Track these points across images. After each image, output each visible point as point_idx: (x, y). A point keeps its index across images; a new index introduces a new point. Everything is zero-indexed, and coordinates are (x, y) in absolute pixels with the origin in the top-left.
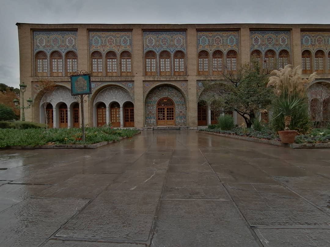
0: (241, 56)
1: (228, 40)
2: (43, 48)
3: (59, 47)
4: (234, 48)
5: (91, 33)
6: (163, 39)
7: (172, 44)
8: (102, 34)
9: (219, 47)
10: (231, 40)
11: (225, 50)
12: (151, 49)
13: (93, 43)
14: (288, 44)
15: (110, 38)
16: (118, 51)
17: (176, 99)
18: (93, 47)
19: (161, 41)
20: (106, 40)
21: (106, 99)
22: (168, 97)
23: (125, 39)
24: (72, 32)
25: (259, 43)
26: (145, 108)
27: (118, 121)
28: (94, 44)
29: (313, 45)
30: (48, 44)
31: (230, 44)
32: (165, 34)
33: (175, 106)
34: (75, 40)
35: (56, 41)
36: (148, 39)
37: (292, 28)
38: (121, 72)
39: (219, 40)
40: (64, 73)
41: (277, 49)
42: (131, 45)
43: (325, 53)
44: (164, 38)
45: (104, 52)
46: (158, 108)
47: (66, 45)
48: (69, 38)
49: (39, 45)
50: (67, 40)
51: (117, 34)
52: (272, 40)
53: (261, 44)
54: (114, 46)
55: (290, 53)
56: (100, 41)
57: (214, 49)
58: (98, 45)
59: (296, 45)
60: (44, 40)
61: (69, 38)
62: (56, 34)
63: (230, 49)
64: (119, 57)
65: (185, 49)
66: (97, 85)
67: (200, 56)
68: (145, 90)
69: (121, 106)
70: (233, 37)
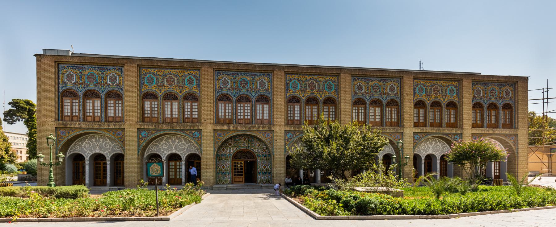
0: (340, 104)
4: (332, 95)
5: (143, 70)
6: (242, 81)
9: (314, 93)
10: (328, 86)
11: (321, 97)
12: (225, 91)
13: (145, 82)
14: (398, 94)
15: (170, 76)
17: (257, 151)
18: (146, 87)
19: (239, 83)
22: (248, 149)
23: (190, 79)
24: (116, 67)
25: (363, 91)
26: (217, 161)
27: (178, 177)
28: (147, 83)
29: (427, 95)
31: (327, 90)
32: (244, 75)
33: (256, 159)
36: (221, 80)
37: (403, 75)
38: (184, 119)
39: (314, 85)
40: (103, 118)
41: (384, 98)
42: (198, 85)
43: (443, 104)
45: (161, 94)
46: (233, 161)
47: (106, 83)
48: (111, 75)
50: (109, 76)
51: (179, 72)
52: (379, 88)
53: (365, 92)
54: (175, 87)
55: (400, 104)
56: (155, 80)
57: (308, 95)
58: (153, 85)
59: (408, 95)
60: (74, 75)
61: (111, 75)
62: (92, 69)
63: (327, 96)
64: (182, 99)
65: (271, 93)
67: (289, 103)
68: (217, 141)
69: (184, 158)
70: (331, 83)
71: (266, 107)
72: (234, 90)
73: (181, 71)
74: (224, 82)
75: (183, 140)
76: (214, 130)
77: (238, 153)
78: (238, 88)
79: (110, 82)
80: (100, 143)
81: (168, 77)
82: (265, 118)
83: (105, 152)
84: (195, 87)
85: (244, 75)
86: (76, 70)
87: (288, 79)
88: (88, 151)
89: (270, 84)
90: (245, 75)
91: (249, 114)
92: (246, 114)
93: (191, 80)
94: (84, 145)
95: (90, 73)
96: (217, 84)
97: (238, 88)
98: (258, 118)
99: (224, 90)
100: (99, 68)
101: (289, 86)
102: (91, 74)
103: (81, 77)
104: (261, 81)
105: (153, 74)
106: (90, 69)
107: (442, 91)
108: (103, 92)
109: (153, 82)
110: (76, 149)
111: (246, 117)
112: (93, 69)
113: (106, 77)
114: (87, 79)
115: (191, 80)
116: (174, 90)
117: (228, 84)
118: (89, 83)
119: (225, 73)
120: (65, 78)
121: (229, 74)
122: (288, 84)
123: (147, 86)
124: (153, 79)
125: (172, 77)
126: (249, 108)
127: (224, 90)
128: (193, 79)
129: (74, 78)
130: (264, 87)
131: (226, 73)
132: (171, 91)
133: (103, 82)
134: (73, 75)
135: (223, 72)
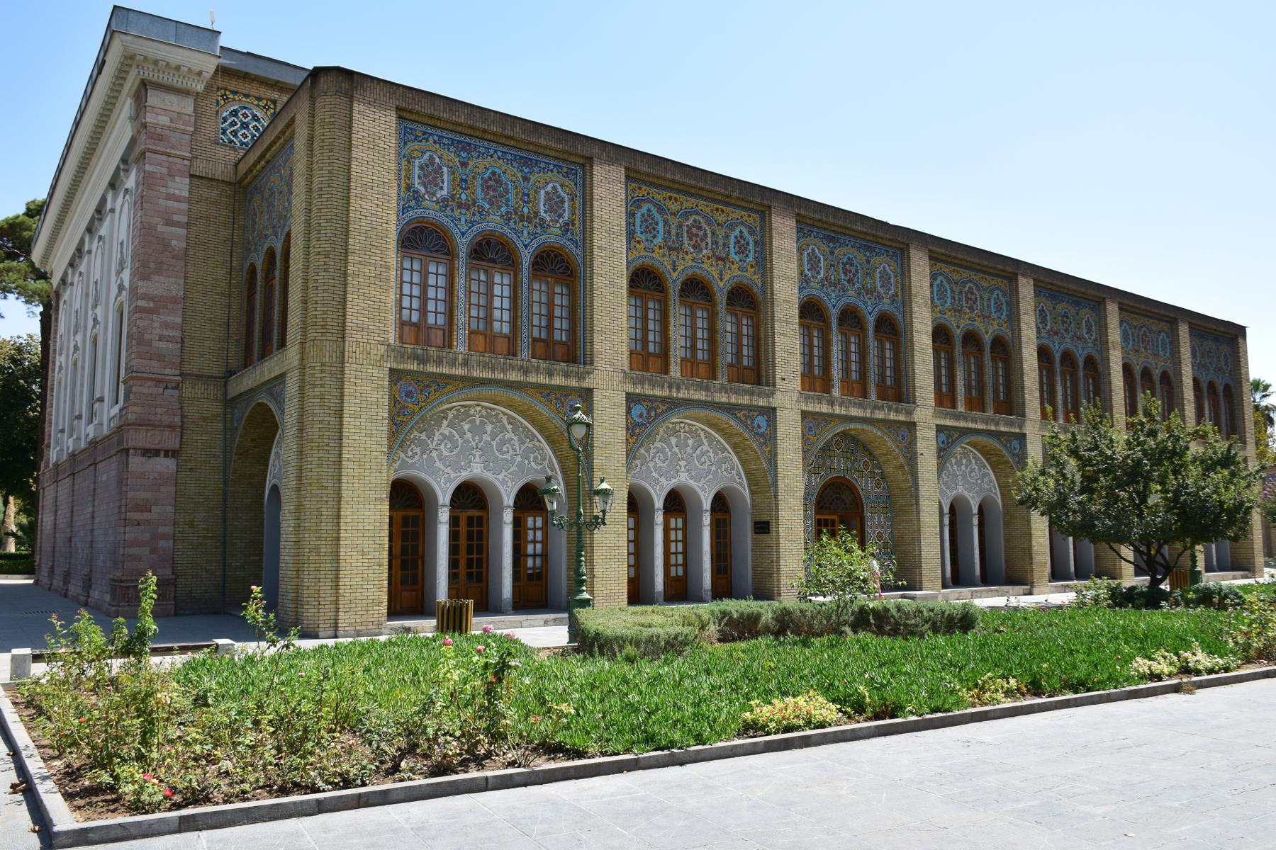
1: (992, 300)
2: (437, 207)
3: (507, 217)
7: (869, 286)
8: (670, 198)
9: (975, 320)
13: (638, 229)
16: (721, 279)
18: (638, 246)
20: (680, 226)
21: (655, 474)
30: (464, 197)
34: (572, 200)
35: (495, 190)
37: (1104, 296)
39: (973, 297)
45: (675, 275)
47: (536, 214)
49: (422, 190)
50: (542, 192)
54: (708, 258)
56: (660, 227)
60: (445, 169)
64: (724, 302)
65: (901, 309)
66: (653, 414)
73: (720, 207)
74: (811, 259)
75: (705, 441)
77: (826, 489)
79: (545, 212)
80: (486, 437)
81: (690, 222)
83: (500, 477)
86: (449, 149)
88: (449, 470)
93: (743, 242)
94: (437, 445)
95: (490, 171)
100: (515, 158)
102: (494, 173)
103: (466, 181)
105: (655, 205)
106: (492, 156)
107: (1153, 345)
108: (526, 246)
109: (656, 232)
110: (410, 461)
112: (499, 158)
113: (535, 192)
114: (483, 191)
116: (704, 266)
118: (488, 206)
120: (416, 177)
123: (642, 246)
124: (657, 223)
125: (700, 223)
129: (443, 182)
132: (699, 272)
133: (526, 210)
134: (440, 168)
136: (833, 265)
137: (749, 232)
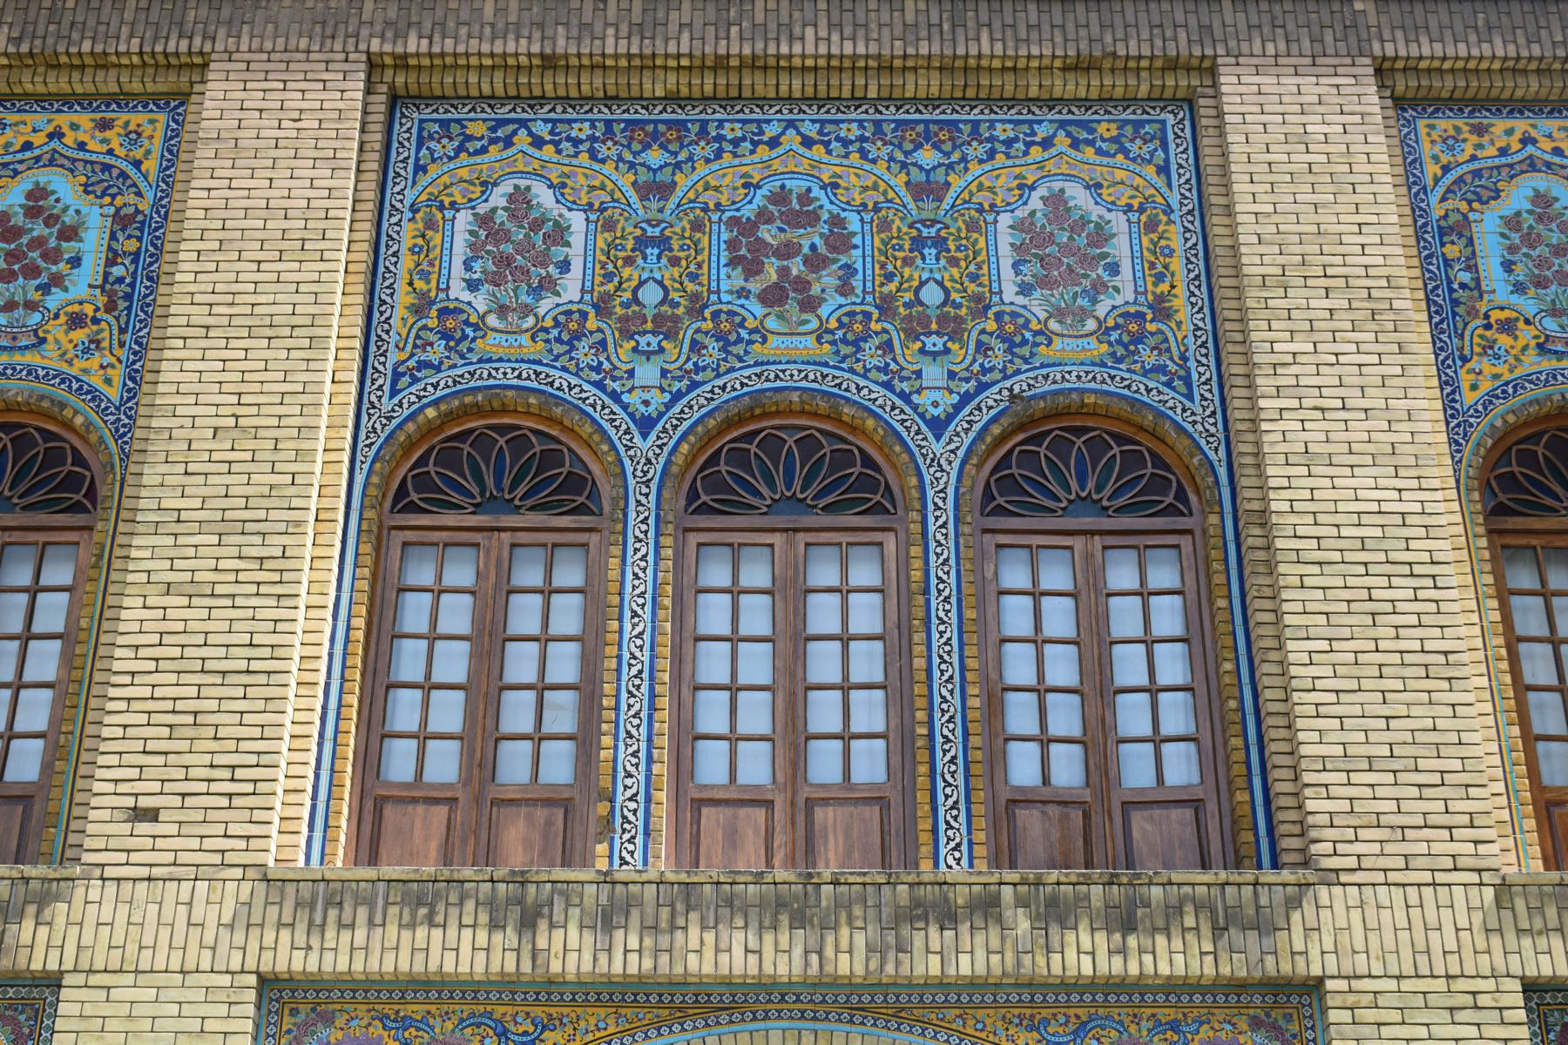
6: (763, 216)
23: (32, 212)
32: (791, 139)
36: (464, 219)
44: (780, 197)
71: (1144, 594)
72: (649, 341)
76: (267, 983)
78: (697, 307)
82: (1136, 770)
84: (76, 321)
85: (791, 139)
87: (1432, 169)
89: (1177, 242)
90: (808, 142)
91: (870, 712)
92: (824, 712)
93: (39, 229)
96: (407, 262)
97: (696, 310)
98: (1023, 767)
99: (491, 343)
101: (1472, 267)
104: (1035, 202)
111: (824, 764)
115: (39, 229)
117: (565, 266)
119: (523, 123)
121: (582, 131)
122: (1459, 229)
126: (866, 614)
127: (491, 343)
128: (68, 219)
130: (1098, 288)
131: (542, 130)
135: (503, 112)
136: (663, 242)
137: (87, 189)
